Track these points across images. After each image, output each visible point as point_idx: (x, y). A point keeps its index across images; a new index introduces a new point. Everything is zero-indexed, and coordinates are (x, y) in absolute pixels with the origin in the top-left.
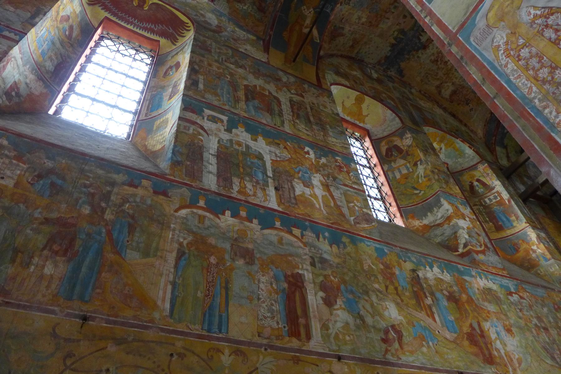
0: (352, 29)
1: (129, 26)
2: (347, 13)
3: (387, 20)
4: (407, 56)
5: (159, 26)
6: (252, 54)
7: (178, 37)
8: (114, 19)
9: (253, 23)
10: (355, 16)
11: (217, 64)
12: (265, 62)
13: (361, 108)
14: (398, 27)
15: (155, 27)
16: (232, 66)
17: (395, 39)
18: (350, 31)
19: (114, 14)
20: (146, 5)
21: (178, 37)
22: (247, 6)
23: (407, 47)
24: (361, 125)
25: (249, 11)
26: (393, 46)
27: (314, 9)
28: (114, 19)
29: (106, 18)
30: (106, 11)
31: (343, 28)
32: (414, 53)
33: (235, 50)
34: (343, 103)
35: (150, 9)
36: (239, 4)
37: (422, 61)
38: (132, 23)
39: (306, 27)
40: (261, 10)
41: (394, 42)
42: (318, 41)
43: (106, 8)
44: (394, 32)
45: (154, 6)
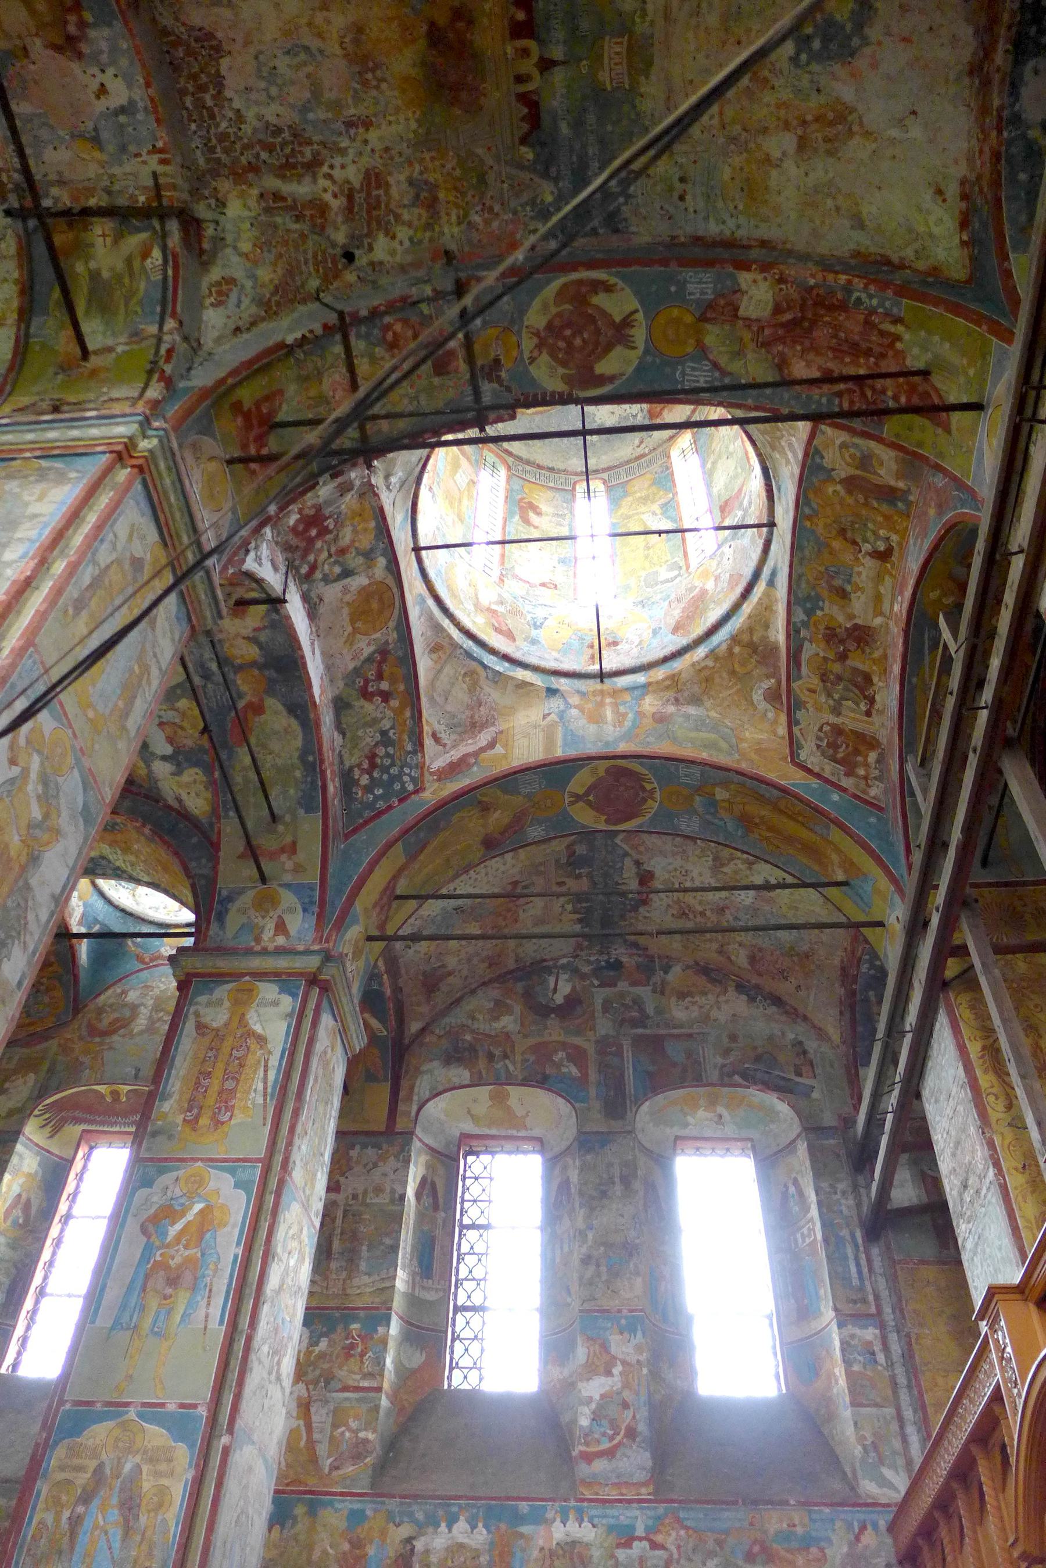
1: (117, 1129)
13: (509, 1108)
19: (91, 1122)
24: (523, 1133)
29: (84, 1131)
34: (469, 1112)
35: (128, 1098)
38: (115, 1123)
43: (77, 1121)
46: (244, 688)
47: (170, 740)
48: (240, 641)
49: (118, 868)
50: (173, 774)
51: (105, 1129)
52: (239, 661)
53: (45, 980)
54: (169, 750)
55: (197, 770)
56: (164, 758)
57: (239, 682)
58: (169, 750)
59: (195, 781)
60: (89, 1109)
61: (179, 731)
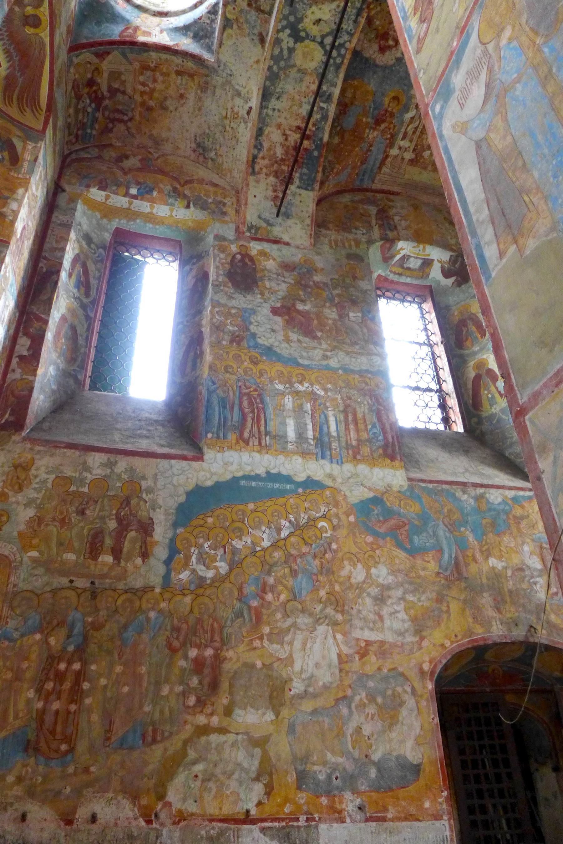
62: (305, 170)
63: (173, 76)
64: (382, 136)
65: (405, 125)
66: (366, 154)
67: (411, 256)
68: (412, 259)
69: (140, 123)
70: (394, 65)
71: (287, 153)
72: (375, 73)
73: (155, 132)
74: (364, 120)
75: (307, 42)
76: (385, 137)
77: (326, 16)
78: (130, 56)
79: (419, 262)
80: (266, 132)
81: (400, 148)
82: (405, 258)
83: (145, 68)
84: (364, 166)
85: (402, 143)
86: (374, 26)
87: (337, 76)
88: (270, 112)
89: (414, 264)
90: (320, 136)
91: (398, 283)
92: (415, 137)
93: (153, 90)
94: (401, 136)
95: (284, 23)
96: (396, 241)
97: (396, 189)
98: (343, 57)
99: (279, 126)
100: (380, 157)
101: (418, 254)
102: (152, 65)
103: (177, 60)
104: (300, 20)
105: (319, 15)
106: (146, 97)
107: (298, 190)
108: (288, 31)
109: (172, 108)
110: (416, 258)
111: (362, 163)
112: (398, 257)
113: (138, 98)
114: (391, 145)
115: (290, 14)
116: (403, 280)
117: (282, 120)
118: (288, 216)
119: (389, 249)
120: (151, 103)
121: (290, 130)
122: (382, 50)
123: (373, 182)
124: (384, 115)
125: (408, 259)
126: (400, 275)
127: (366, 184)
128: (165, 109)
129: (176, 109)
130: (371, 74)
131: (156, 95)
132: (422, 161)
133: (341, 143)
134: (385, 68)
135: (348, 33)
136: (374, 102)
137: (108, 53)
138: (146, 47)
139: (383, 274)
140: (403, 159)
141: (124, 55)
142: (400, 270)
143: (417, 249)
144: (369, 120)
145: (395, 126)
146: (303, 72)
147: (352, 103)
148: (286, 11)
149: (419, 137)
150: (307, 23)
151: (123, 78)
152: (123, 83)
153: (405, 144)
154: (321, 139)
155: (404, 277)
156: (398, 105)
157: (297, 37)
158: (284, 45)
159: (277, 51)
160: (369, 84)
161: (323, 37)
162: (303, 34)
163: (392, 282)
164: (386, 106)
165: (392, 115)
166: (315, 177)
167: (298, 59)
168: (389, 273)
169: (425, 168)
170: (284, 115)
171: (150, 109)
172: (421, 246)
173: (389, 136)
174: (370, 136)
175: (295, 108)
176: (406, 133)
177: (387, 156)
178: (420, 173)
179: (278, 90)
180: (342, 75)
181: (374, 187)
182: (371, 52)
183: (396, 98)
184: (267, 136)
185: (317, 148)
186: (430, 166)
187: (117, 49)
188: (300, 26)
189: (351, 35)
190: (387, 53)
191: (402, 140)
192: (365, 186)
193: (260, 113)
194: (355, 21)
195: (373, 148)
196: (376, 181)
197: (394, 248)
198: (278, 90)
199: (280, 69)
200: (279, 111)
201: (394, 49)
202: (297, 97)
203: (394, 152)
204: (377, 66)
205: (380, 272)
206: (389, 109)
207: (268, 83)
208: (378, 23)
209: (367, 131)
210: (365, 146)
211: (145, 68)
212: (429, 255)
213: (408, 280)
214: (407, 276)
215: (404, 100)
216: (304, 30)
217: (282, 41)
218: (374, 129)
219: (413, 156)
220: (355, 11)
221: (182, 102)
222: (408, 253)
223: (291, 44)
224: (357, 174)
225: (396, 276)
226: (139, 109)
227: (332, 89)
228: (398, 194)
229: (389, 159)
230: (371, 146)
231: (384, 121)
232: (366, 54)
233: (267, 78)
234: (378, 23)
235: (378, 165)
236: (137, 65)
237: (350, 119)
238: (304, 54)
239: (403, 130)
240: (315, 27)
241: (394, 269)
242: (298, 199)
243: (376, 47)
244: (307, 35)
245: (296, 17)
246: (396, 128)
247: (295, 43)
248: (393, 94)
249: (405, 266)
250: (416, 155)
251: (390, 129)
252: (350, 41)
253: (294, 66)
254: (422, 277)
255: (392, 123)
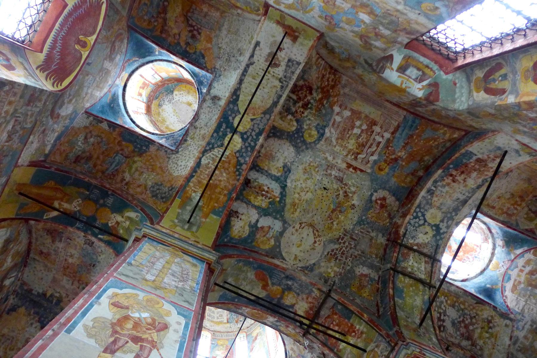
0: (60, 250)
1: (57, 26)
2: (76, 243)
3: (70, 282)
4: (32, 312)
5: (59, 55)
6: (27, 149)
7: (46, 73)
8: (66, 12)
9: (64, 150)
10: (73, 251)
11: (12, 111)
12: (17, 162)
14: (64, 295)
15: (58, 52)
16: (10, 127)
17: (52, 295)
18: (58, 248)
19: (70, 14)
20: (80, 47)
21: (46, 73)
22: (81, 145)
23: (42, 309)
25: (77, 147)
26: (44, 295)
27: (79, 211)
28: (66, 12)
29: (66, 5)
30: (73, 6)
31: (61, 241)
32: (37, 319)
33: (31, 131)
36: (83, 138)
37: (27, 329)
39: (60, 204)
40: (77, 159)
41: (48, 295)
42: (45, 218)
44: (59, 293)
45: (79, 55)
46: (275, 288)
47: (262, 228)
48: (294, 302)
49: (213, 148)
50: (250, 222)
51: (60, 20)
52: (286, 293)
53: (156, 24)
54: (259, 225)
55: (247, 234)
56: (257, 221)
57: (278, 287)
58: (259, 225)
59: (244, 232)
60: (81, 19)
61: (264, 234)
62: (464, 161)
63: (497, 207)
64: (394, 150)
65: (377, 152)
66: (408, 142)
67: (414, 80)
68: (414, 77)
69: (531, 193)
70: (379, 189)
71: (470, 172)
72: (390, 187)
73: (526, 185)
74: (404, 164)
75: (433, 224)
76: (393, 149)
77: (421, 235)
78: (514, 223)
79: (408, 72)
80: (475, 185)
81: (383, 137)
82: (420, 80)
83: (510, 215)
84: (411, 133)
85: (381, 140)
86: (388, 213)
87: (420, 201)
88: (467, 194)
89: (413, 72)
90: (443, 174)
91: (432, 60)
92: (371, 141)
93: (512, 205)
94: (381, 145)
95: (442, 236)
96: (423, 98)
97: (389, 105)
98: (415, 211)
99: (466, 186)
100: (397, 135)
101: (408, 80)
102: (505, 215)
103: (491, 213)
104: (434, 236)
105: (425, 237)
106: (519, 203)
107: (477, 154)
108: (441, 231)
109: (509, 194)
110: (410, 77)
111: (412, 136)
112: (425, 83)
113: (524, 204)
114: (388, 141)
115: (439, 240)
116: (426, 61)
117: (462, 188)
118: (499, 148)
119: (430, 94)
120: (518, 199)
121: (460, 182)
122: (384, 199)
123: (405, 116)
124: (391, 163)
125: (417, 78)
126: (427, 67)
127: (411, 117)
128: (513, 195)
129: (506, 193)
130: (393, 187)
131: (513, 202)
132: (368, 123)
133: (425, 156)
134: (384, 189)
135: (410, 224)
136: (394, 171)
137: (527, 230)
138: (503, 223)
139: (442, 73)
140: (381, 128)
141: (517, 225)
142: (427, 71)
143: (407, 85)
144: (401, 163)
145: (385, 154)
146: (439, 208)
147: (408, 174)
148: (440, 242)
149: (368, 140)
150: (431, 233)
151: (525, 216)
152: (527, 214)
153: (379, 139)
154: (443, 172)
155: (425, 63)
156: (380, 166)
157: (437, 228)
158: (445, 224)
159: (450, 222)
160: (395, 182)
161: (424, 224)
162: (434, 228)
163: (436, 63)
164: (388, 167)
165: (385, 161)
166: (460, 155)
167: (440, 216)
168: (436, 71)
169: (367, 116)
170: (460, 190)
171: (521, 197)
172: (404, 86)
173: (390, 148)
174: (403, 153)
175: (451, 192)
176: (378, 146)
177: (393, 133)
178: (370, 113)
179: (457, 203)
180: (418, 201)
181: (405, 113)
182: (391, 199)
183: (381, 170)
184: (476, 183)
185: (449, 168)
186: (363, 117)
187: (520, 229)
188: (435, 232)
189: (409, 223)
190: (382, 196)
191: (381, 142)
192: (412, 116)
193: (473, 195)
194: (407, 230)
195: (403, 144)
196: (403, 117)
197: (427, 93)
198: (457, 203)
199: (451, 213)
200: (461, 193)
201: (378, 198)
202: (447, 197)
203: (387, 135)
204: (389, 191)
205: (444, 77)
206: (386, 165)
207: (461, 208)
208: (385, 214)
209: (404, 157)
210: (408, 148)
211: (510, 215)
212: (399, 77)
213: (422, 59)
214: (422, 63)
215: (376, 167)
216: (433, 230)
217: (445, 227)
218: (400, 157)
219: (374, 127)
220: (407, 236)
221: (501, 195)
222: (415, 83)
223: (441, 224)
224: (417, 129)
225: (431, 66)
226: (526, 199)
227: (425, 195)
228: (388, 101)
229: (391, 130)
230: (404, 147)
231: (392, 159)
232: (393, 198)
233: (460, 210)
234: (385, 214)
235: (400, 130)
236: (514, 218)
237: (413, 167)
238: (436, 218)
239: (379, 149)
240: (427, 231)
241: (432, 73)
242: (481, 151)
243: (388, 201)
244: (432, 228)
245: (436, 238)
246: (384, 152)
247: (439, 225)
248: (383, 173)
249: (420, 73)
250: (371, 128)
251: (389, 153)
252: (410, 219)
253: (443, 213)
254: (409, 57)
255: (387, 157)
